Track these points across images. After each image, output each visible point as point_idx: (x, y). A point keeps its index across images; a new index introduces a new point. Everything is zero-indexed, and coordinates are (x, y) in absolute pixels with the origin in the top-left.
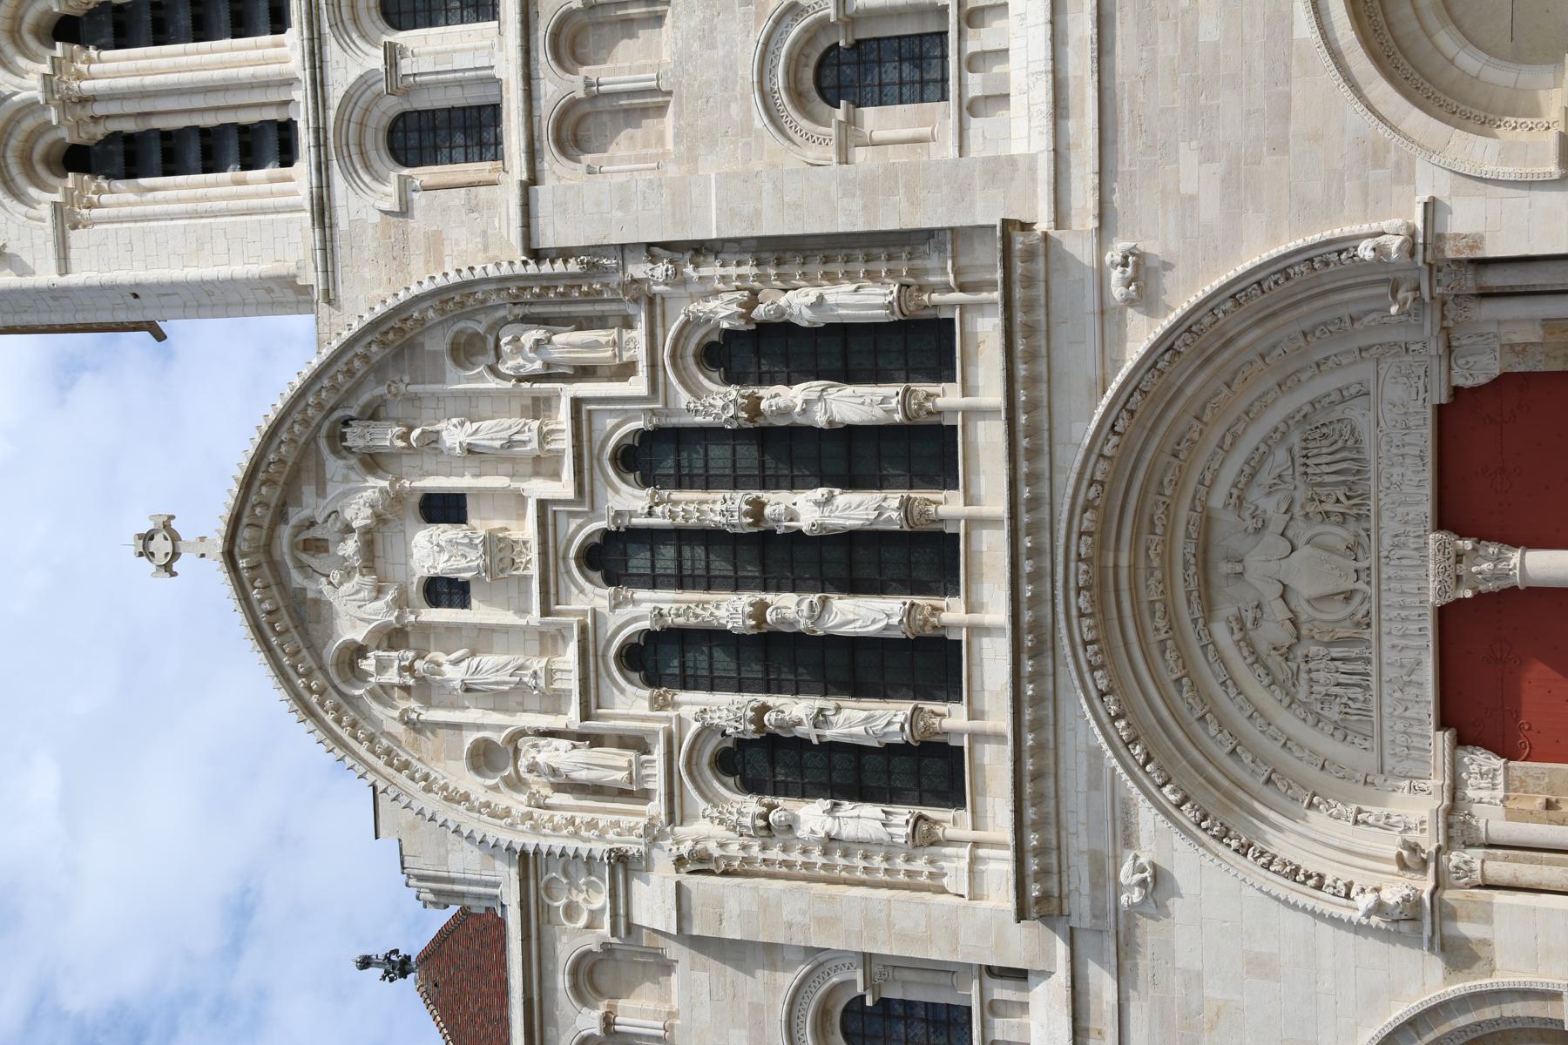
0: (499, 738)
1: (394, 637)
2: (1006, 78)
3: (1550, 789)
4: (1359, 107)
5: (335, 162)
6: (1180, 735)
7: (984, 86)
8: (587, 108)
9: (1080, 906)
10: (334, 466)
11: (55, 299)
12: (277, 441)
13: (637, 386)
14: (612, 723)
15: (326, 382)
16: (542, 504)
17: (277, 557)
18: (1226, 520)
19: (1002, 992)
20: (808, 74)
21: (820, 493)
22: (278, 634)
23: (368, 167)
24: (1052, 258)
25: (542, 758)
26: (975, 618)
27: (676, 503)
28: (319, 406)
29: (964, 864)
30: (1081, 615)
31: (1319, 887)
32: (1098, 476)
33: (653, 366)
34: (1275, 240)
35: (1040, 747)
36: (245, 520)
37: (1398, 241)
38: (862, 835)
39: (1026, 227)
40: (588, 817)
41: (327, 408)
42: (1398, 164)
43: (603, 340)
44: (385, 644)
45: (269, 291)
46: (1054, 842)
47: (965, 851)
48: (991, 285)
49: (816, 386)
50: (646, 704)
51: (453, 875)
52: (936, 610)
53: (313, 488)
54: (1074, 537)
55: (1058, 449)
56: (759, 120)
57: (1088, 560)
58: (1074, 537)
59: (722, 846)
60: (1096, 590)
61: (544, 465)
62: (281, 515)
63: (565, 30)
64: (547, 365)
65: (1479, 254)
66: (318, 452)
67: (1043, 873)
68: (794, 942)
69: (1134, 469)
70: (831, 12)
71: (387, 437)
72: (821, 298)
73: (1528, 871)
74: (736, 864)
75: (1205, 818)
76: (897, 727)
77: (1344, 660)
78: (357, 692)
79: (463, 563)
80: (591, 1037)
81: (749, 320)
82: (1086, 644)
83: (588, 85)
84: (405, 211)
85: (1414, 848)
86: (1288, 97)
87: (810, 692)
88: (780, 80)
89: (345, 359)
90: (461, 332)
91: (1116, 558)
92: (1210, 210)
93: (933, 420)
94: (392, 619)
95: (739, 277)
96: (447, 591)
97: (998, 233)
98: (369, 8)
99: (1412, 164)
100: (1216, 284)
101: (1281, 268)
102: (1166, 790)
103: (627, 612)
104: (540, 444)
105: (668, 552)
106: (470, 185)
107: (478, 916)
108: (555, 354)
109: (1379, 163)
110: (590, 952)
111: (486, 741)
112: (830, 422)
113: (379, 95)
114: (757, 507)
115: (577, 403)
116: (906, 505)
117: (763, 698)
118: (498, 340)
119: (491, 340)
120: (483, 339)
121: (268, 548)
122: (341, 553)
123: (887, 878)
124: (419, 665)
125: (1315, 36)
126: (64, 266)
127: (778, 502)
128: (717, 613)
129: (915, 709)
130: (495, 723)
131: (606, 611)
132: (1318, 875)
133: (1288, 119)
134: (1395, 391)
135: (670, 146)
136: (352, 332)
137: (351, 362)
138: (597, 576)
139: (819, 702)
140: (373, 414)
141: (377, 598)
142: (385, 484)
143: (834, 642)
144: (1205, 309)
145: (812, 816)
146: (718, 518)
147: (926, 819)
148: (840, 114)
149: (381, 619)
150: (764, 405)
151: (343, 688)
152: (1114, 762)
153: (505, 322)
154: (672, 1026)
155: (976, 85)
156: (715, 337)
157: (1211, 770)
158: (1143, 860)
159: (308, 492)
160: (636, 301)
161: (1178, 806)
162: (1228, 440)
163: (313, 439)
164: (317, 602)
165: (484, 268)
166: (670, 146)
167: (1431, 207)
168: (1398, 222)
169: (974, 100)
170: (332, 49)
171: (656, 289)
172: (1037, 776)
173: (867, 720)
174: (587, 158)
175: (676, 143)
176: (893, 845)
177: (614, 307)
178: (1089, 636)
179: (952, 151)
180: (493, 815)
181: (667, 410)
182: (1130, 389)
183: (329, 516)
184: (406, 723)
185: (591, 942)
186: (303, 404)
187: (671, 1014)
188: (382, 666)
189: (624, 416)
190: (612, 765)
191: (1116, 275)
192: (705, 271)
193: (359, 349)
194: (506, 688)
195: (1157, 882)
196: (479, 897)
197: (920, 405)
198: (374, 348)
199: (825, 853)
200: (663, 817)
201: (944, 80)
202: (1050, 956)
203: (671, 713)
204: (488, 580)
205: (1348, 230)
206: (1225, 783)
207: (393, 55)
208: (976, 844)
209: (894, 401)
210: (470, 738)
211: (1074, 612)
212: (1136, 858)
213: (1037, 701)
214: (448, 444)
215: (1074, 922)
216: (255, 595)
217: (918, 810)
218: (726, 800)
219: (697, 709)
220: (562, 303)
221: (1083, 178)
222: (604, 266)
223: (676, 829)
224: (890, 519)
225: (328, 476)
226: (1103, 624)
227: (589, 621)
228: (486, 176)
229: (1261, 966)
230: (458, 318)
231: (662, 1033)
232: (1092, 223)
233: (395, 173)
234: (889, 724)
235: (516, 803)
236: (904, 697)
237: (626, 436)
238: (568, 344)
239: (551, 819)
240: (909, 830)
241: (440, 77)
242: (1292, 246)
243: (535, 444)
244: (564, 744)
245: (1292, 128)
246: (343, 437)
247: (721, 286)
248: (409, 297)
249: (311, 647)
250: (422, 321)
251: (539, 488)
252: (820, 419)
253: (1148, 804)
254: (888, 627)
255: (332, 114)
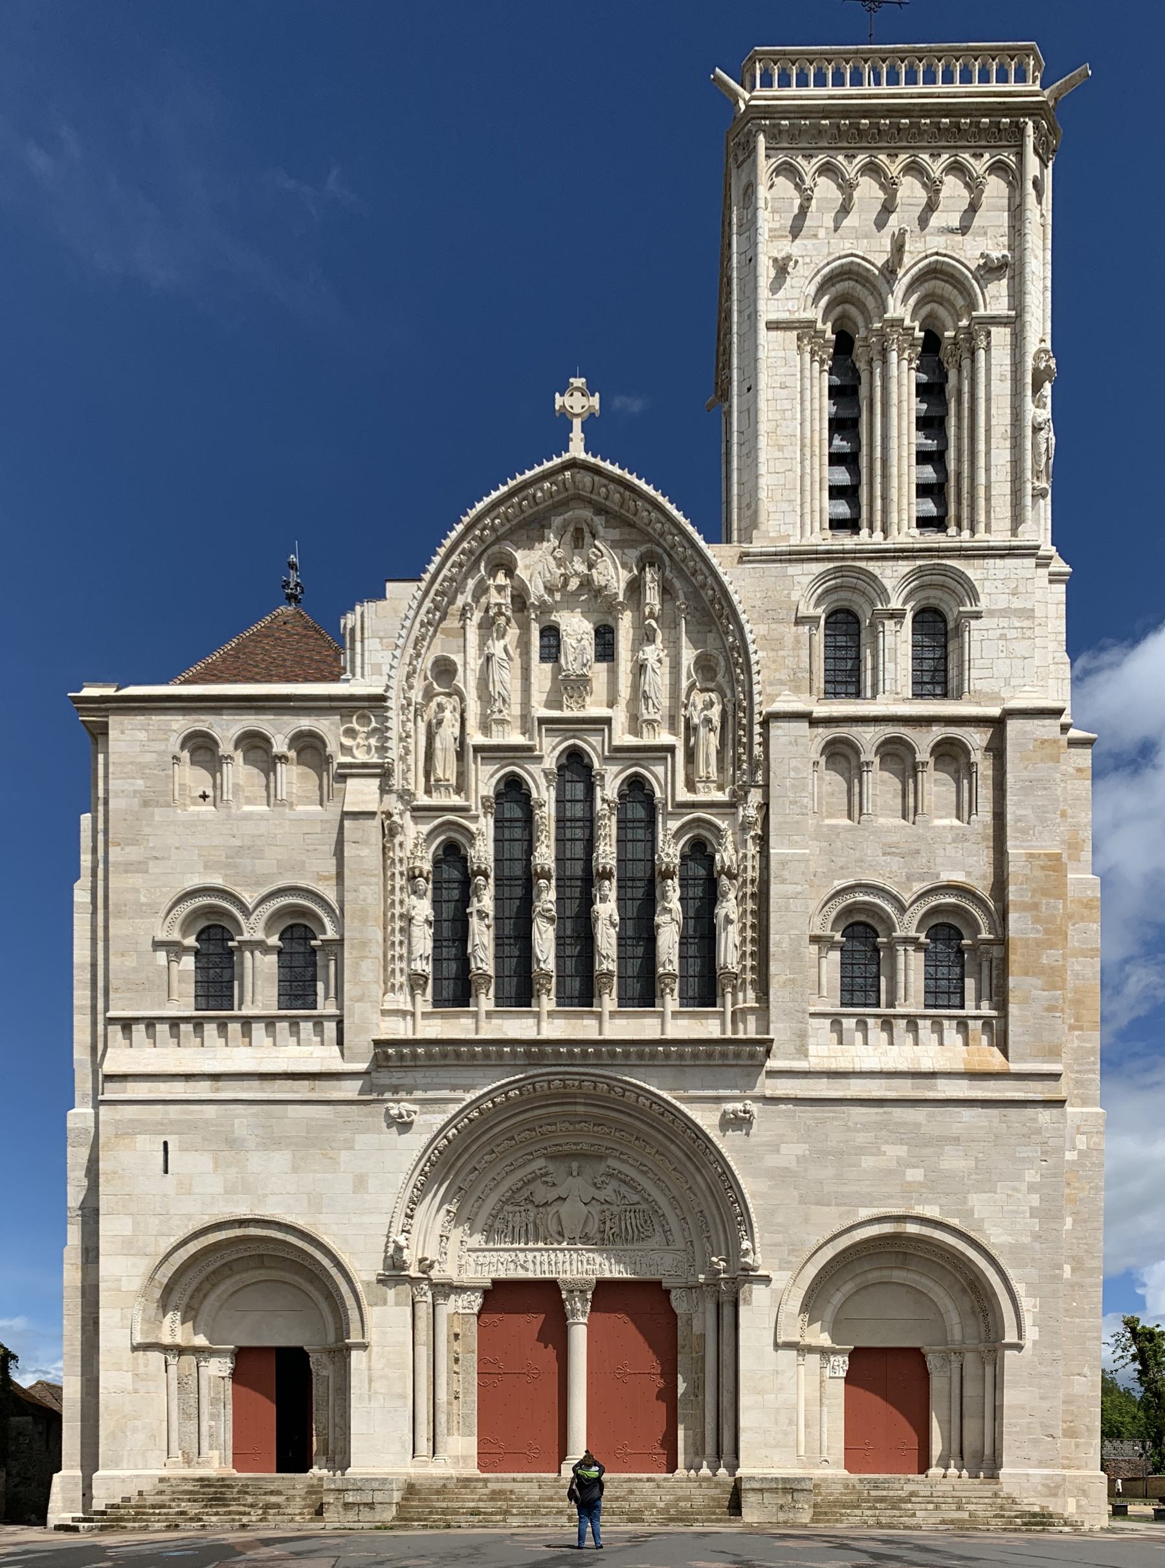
0: (459, 681)
1: (520, 600)
2: (852, 1043)
3: (464, 1335)
4: (821, 1242)
5: (831, 565)
6: (484, 1139)
7: (848, 1030)
8: (854, 763)
9: (383, 1078)
10: (633, 554)
11: (749, 317)
12: (650, 508)
13: (683, 795)
14: (473, 766)
15: (689, 552)
16: (608, 721)
17: (572, 504)
18: (602, 1168)
19: (330, 1028)
20: (862, 918)
21: (616, 918)
22: (520, 504)
23: (827, 592)
24: (750, 1069)
25: (447, 714)
26: (544, 1016)
27: (609, 819)
28: (673, 546)
29: (402, 1007)
30: (549, 1082)
31: (407, 1216)
32: (627, 1093)
33: (694, 805)
34: (753, 1196)
35: (474, 1056)
36: (597, 478)
37: (750, 1262)
38: (414, 941)
39: (768, 1053)
40: (412, 748)
41: (672, 553)
42: (790, 1262)
43: (710, 770)
44: (515, 593)
45: (749, 506)
46: (419, 1063)
47: (409, 1007)
48: (735, 1032)
49: (680, 917)
50: (485, 794)
51: (366, 641)
52: (549, 991)
53: (617, 537)
54: (593, 1079)
55: (642, 1070)
56: (839, 884)
57: (580, 1087)
58: (593, 1079)
59: (401, 845)
60: (562, 1091)
61: (636, 724)
62: (600, 510)
63: (902, 748)
64: (696, 728)
65: (741, 1302)
66: (642, 543)
67: (401, 1057)
68: (346, 893)
69: (630, 1115)
70: (898, 933)
71: (652, 597)
72: (731, 922)
73: (423, 1324)
74: (391, 854)
75: (440, 1152)
76: (480, 965)
77: (527, 1230)
78: (482, 569)
79: (571, 658)
80: (271, 746)
81: (722, 872)
82: (533, 1084)
83: (867, 764)
84: (799, 621)
85: (431, 1266)
86: (828, 1205)
87: (496, 907)
88: (861, 897)
89: (704, 568)
90: (717, 664)
91: (580, 1104)
92: (771, 1161)
93: (658, 993)
94: (532, 600)
95: (746, 867)
96: (551, 633)
97: (766, 1037)
98: (928, 598)
99: (788, 1269)
100: (732, 1164)
101: (741, 1199)
102: (454, 1131)
103: (543, 782)
104: (646, 721)
105: (578, 810)
106: (811, 672)
107: (337, 660)
108: (702, 731)
109: (791, 1252)
110: (325, 745)
111: (455, 671)
112: (658, 926)
113: (873, 604)
114: (606, 875)
115: (671, 749)
116: (609, 974)
117: (492, 875)
118: (712, 691)
119: (712, 685)
120: (713, 679)
121: (578, 498)
122: (575, 559)
123: (389, 957)
124: (502, 620)
125: (859, 1220)
126: (773, 326)
127: (610, 889)
128: (544, 846)
129: (490, 977)
130: (468, 680)
131: (542, 766)
132: (411, 1217)
133: (817, 1204)
134: (669, 1260)
135: (828, 822)
136: (722, 575)
137: (703, 574)
138: (564, 761)
139: (492, 914)
140: (666, 591)
141: (546, 587)
142: (621, 598)
143: (529, 922)
144: (718, 1157)
145: (423, 908)
146: (601, 848)
147: (426, 982)
148: (838, 937)
149: (532, 589)
150: (669, 882)
151: (485, 556)
152: (469, 1100)
153: (723, 695)
154: (284, 805)
155: (849, 1024)
156: (709, 849)
157: (466, 1156)
158: (414, 1116)
159: (615, 534)
160: (733, 794)
161: (445, 1137)
162: (644, 1169)
163: (651, 540)
164: (542, 539)
165: (758, 683)
166: (828, 822)
167: (766, 1280)
168: (760, 1262)
169: (840, 1023)
170: (905, 567)
171: (741, 809)
172: (458, 1055)
173: (485, 947)
174: (823, 761)
175: (828, 825)
176: (409, 961)
177: (730, 778)
178: (537, 1086)
179: (812, 1010)
180: (409, 676)
181: (668, 816)
182: (676, 1113)
183: (599, 550)
184: (464, 608)
185: (332, 748)
186: (675, 532)
187: (291, 804)
188: (500, 589)
189: (663, 782)
190: (446, 769)
191: (739, 1106)
192: (750, 842)
193: (710, 580)
194: (491, 688)
195: (404, 1126)
196: (353, 661)
197: (667, 985)
198: (710, 592)
199: (402, 916)
200: (415, 803)
201: (852, 1005)
202: (352, 1060)
203: (481, 812)
204: (560, 677)
205: (756, 1235)
206: (459, 1164)
207: (897, 616)
208: (413, 1015)
209: (670, 968)
210: (457, 658)
211: (551, 1077)
212: (415, 1112)
213: (501, 1055)
214: (646, 648)
215: (373, 1074)
216: (547, 485)
217: (431, 977)
218: (428, 848)
219: (484, 830)
220: (734, 739)
221: (792, 1088)
222: (756, 772)
223: (408, 813)
224: (601, 963)
225: (626, 551)
226: (547, 1097)
227: (536, 753)
228: (815, 685)
229: (360, 1183)
230: (727, 660)
231: (279, 797)
232: (768, 1093)
233: (821, 612)
234: (482, 960)
235: (417, 696)
236: (496, 970)
237: (651, 784)
238: (710, 742)
239: (409, 720)
240: (420, 972)
241: (881, 653)
242: (750, 1206)
243: (646, 717)
244: (457, 733)
245: (813, 1207)
246: (652, 565)
247: (741, 855)
248: (743, 622)
249: (512, 531)
250: (727, 633)
251: (620, 716)
252: (659, 919)
253: (446, 1120)
254: (538, 961)
255: (862, 564)
